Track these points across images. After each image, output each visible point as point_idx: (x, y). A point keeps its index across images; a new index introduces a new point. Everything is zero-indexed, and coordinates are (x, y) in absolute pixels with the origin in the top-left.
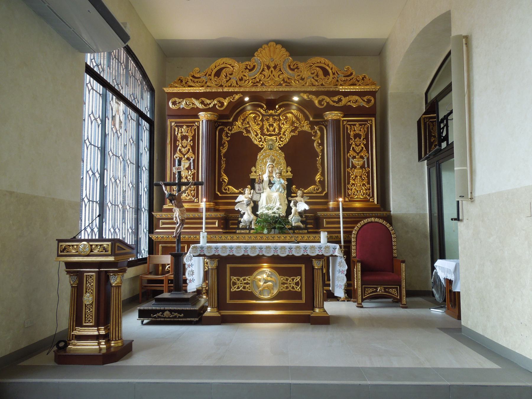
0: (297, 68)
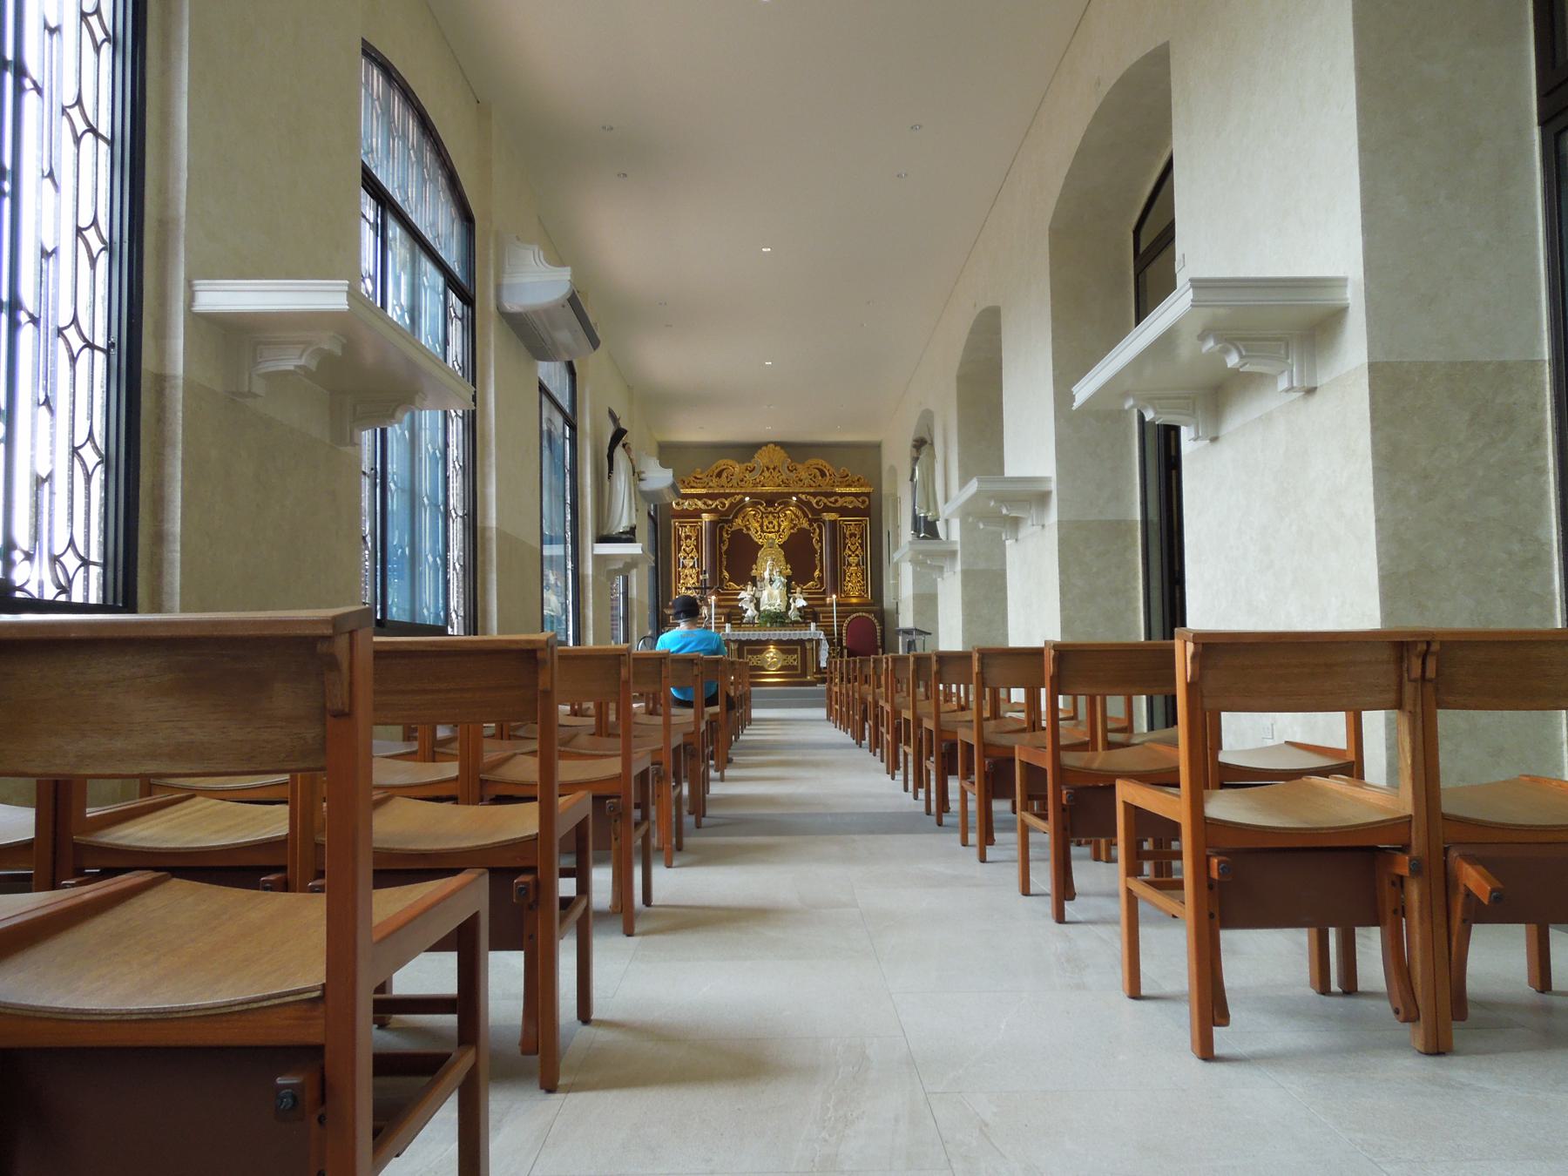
0: (796, 469)
